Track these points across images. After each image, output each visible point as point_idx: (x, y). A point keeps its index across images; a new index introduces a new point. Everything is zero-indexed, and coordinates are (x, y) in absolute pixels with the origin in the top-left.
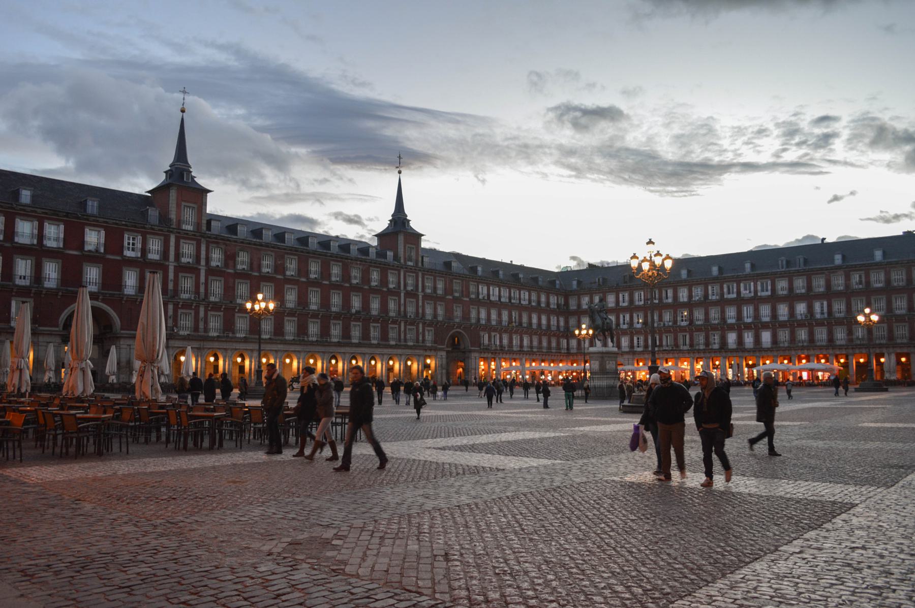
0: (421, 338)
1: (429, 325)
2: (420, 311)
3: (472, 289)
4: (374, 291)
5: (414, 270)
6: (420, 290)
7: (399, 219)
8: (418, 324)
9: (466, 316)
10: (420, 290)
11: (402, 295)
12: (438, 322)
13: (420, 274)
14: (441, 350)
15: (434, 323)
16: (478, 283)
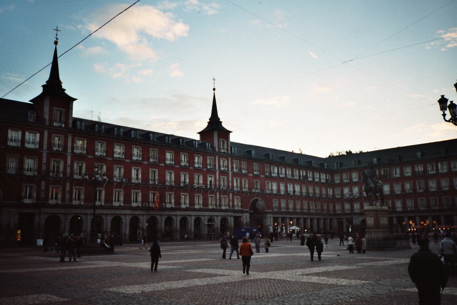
0: (231, 204)
1: (237, 195)
2: (230, 184)
3: (267, 170)
4: (198, 170)
5: (225, 156)
6: (230, 170)
7: (215, 121)
8: (229, 194)
9: (263, 188)
10: (230, 170)
11: (217, 173)
12: (243, 192)
13: (230, 159)
14: (246, 212)
15: (239, 193)
16: (270, 165)
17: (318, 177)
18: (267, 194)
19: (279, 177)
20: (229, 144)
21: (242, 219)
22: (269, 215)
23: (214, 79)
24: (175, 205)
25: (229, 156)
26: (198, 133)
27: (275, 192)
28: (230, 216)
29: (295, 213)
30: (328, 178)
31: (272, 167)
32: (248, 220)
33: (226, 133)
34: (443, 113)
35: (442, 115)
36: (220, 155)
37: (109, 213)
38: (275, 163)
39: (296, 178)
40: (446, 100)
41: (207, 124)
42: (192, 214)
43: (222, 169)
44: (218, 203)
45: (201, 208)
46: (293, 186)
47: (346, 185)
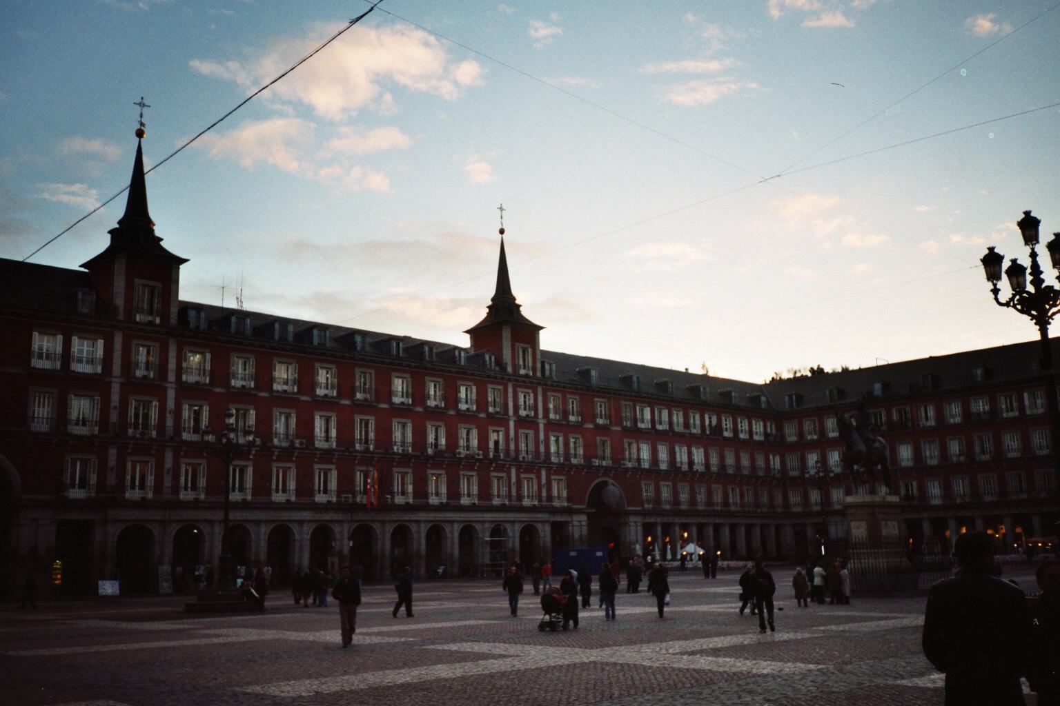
0: (544, 494)
2: (542, 449)
3: (626, 413)
4: (467, 417)
5: (529, 383)
6: (540, 416)
7: (504, 304)
9: (618, 455)
10: (540, 416)
11: (512, 424)
12: (572, 466)
13: (540, 390)
14: (579, 512)
15: (564, 468)
17: (747, 428)
18: (627, 469)
19: (656, 430)
20: (539, 357)
21: (570, 528)
22: (632, 519)
23: (501, 209)
24: (413, 499)
25: (539, 384)
26: (467, 332)
27: (646, 465)
28: (543, 522)
29: (694, 513)
30: (769, 430)
31: (638, 408)
32: (585, 530)
33: (530, 332)
34: (992, 287)
35: (992, 291)
36: (517, 380)
37: (264, 518)
38: (644, 398)
39: (694, 431)
40: (1000, 258)
41: (487, 310)
42: (454, 519)
43: (523, 413)
44: (514, 493)
45: (474, 504)
46: (688, 449)
47: (812, 446)
